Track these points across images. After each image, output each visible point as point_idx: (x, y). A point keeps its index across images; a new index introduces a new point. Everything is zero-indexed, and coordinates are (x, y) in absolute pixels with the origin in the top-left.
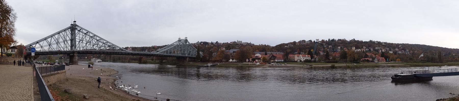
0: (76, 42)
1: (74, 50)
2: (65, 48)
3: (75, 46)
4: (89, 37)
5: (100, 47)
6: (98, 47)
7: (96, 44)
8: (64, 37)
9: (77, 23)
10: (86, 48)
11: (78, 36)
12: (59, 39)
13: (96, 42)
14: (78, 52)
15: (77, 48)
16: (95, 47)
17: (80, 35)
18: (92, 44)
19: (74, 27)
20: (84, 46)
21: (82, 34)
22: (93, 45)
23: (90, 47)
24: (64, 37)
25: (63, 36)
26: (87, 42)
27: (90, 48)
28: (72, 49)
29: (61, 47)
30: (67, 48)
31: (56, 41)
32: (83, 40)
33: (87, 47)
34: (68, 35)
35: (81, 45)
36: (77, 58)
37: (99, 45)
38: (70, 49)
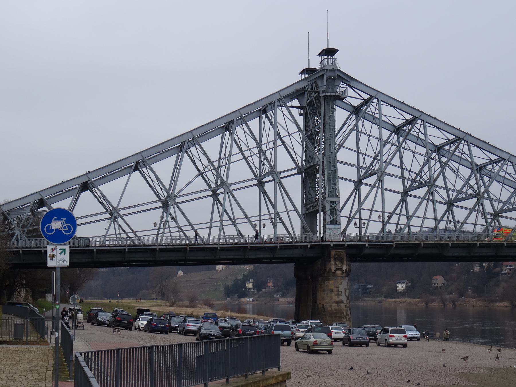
0: (336, 184)
1: (328, 238)
2: (269, 224)
3: (334, 211)
4: (423, 151)
5: (496, 215)
6: (484, 214)
7: (470, 191)
8: (261, 152)
10: (403, 220)
11: (351, 142)
12: (228, 164)
13: (466, 182)
15: (344, 222)
16: (460, 214)
17: (364, 139)
18: (441, 195)
19: (322, 85)
20: (389, 209)
21: (375, 131)
22: (450, 204)
23: (430, 214)
24: (261, 152)
25: (252, 144)
26: (408, 184)
27: (430, 224)
28: (314, 231)
29: (238, 214)
30: (279, 226)
31: (210, 176)
32: (381, 174)
33: (409, 218)
34: (286, 140)
35: (367, 205)
36: (343, 285)
37: (487, 203)
38: (298, 231)
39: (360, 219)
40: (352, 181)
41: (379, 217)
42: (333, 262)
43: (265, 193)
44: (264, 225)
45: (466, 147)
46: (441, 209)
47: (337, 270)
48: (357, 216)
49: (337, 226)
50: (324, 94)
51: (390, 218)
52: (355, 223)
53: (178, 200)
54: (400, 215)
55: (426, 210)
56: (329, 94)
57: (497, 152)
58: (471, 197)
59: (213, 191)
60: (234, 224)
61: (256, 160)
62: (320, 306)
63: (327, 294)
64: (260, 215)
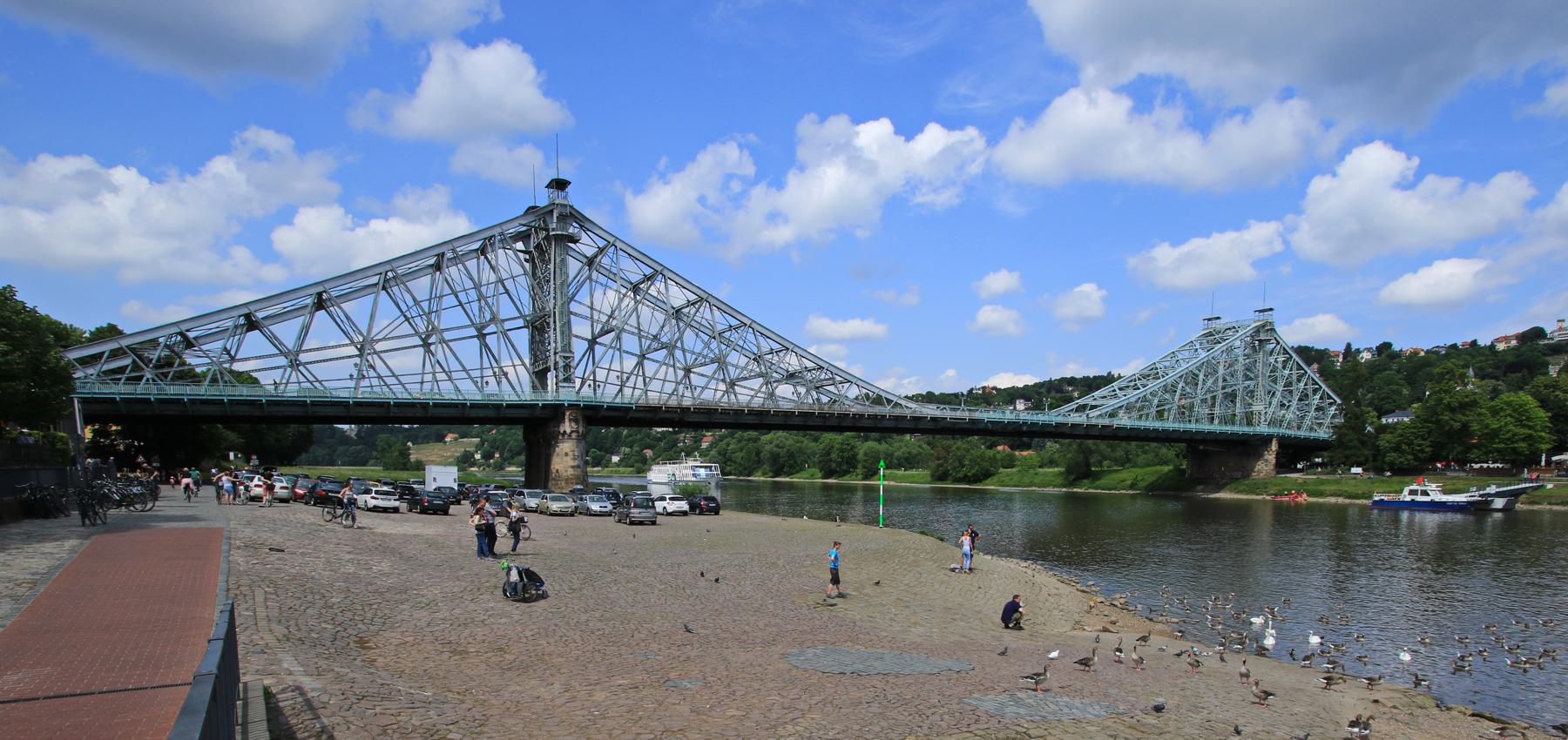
2: (492, 380)
3: (567, 367)
7: (712, 355)
8: (481, 297)
9: (574, 198)
14: (589, 413)
22: (688, 371)
23: (671, 376)
24: (481, 297)
26: (646, 343)
29: (454, 365)
39: (595, 381)
40: (586, 339)
41: (618, 377)
42: (567, 423)
43: (486, 346)
44: (487, 383)
45: (708, 310)
46: (681, 373)
47: (572, 432)
48: (591, 378)
49: (571, 385)
50: (554, 233)
51: (628, 378)
52: (590, 385)
53: (379, 347)
54: (637, 375)
55: (666, 373)
56: (560, 233)
57: (739, 317)
58: (712, 362)
59: (423, 340)
60: (450, 379)
61: (475, 306)
62: (554, 471)
63: (562, 458)
64: (482, 369)
